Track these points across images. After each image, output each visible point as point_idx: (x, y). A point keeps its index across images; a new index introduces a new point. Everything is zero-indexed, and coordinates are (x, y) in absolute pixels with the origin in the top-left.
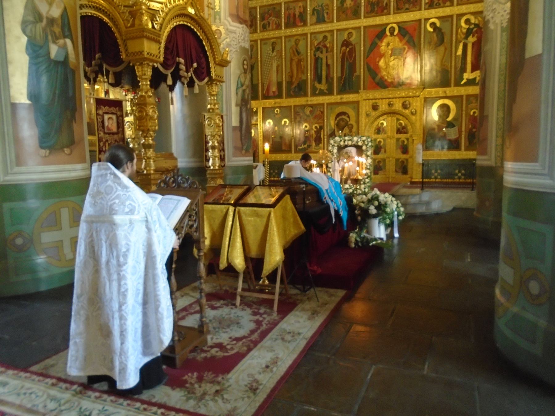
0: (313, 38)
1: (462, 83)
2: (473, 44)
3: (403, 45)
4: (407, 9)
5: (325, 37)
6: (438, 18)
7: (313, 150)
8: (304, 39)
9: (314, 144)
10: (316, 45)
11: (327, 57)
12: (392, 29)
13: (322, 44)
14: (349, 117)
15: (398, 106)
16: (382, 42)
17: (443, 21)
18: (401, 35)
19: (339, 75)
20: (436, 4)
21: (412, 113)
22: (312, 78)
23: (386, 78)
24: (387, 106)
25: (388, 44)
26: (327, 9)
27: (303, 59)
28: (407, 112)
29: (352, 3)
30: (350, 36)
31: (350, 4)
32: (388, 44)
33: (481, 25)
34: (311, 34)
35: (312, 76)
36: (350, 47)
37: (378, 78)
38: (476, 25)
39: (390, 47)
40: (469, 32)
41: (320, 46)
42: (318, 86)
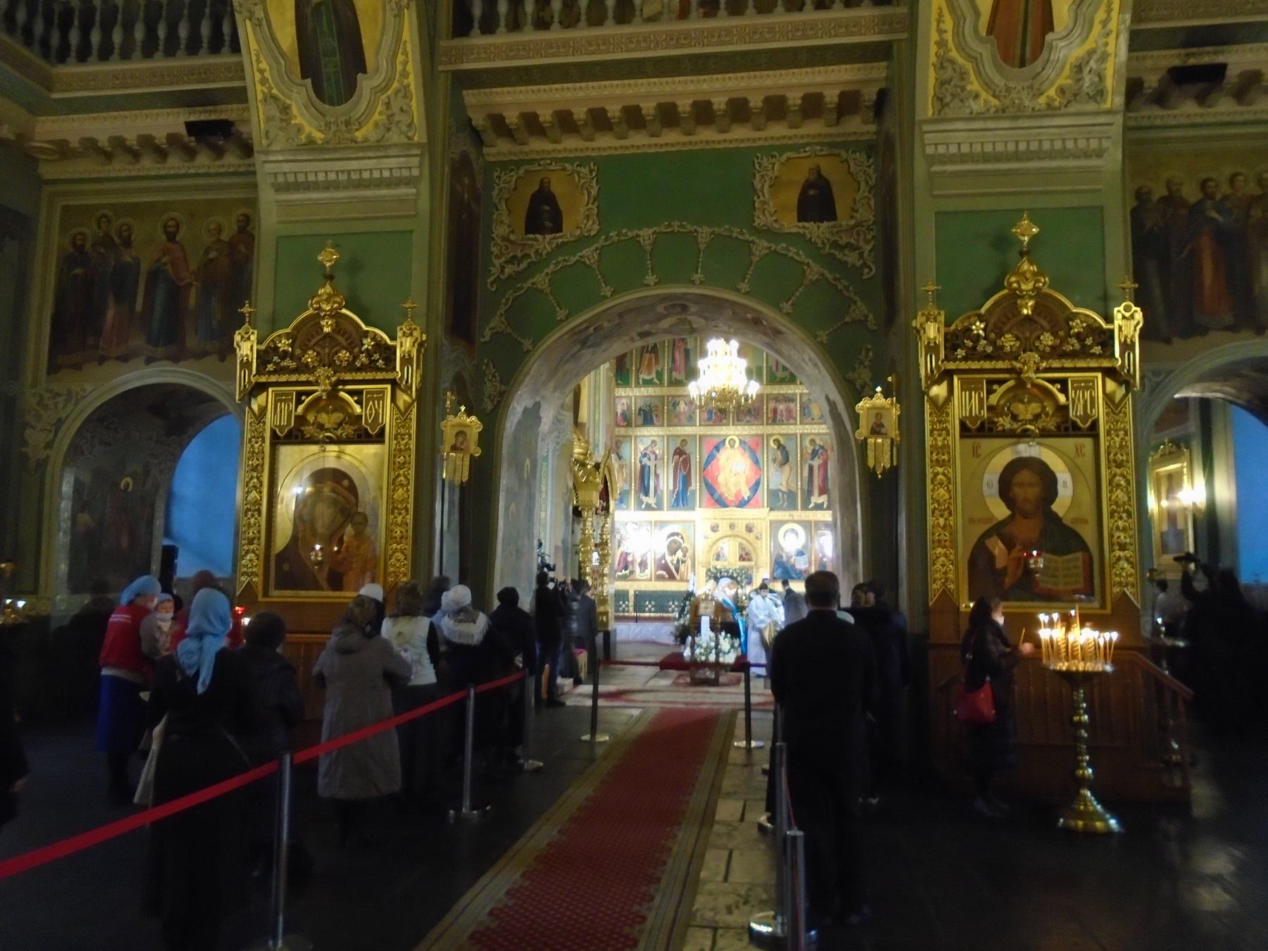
1: (811, 506)
4: (748, 422)
5: (653, 442)
6: (781, 435)
7: (637, 577)
9: (637, 569)
10: (642, 449)
13: (650, 449)
14: (682, 538)
15: (741, 528)
17: (787, 439)
19: (671, 487)
21: (757, 538)
24: (728, 529)
28: (751, 535)
29: (686, 408)
33: (825, 447)
37: (716, 496)
38: (822, 447)
40: (814, 454)
41: (648, 452)
42: (645, 499)
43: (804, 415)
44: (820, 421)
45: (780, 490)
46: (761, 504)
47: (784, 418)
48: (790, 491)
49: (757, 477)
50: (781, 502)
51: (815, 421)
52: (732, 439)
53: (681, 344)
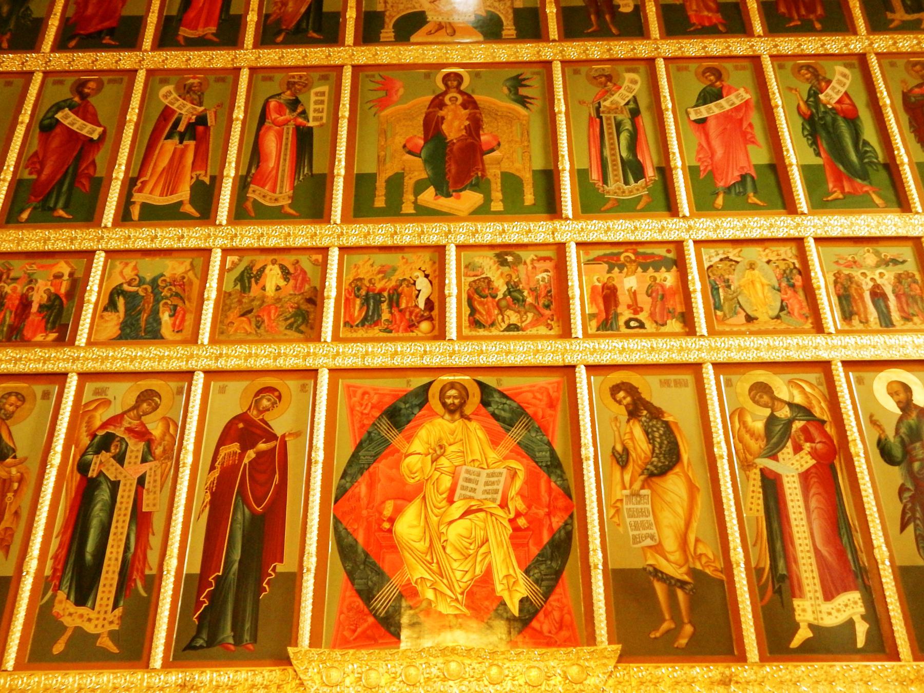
0: (87, 397)
2: (805, 477)
3: (506, 458)
4: (512, 327)
8: (46, 395)
10: (98, 423)
11: (141, 481)
12: (453, 392)
13: (127, 422)
16: (409, 439)
17: (666, 383)
18: (494, 416)
19: (194, 565)
20: (627, 324)
22: (48, 572)
23: (430, 594)
25: (437, 452)
26: (177, 294)
27: (21, 480)
29: (289, 288)
30: (265, 403)
31: (278, 288)
32: (437, 452)
33: (817, 412)
34: (84, 376)
35: (49, 563)
36: (262, 446)
39: (443, 461)
41: (119, 432)
43: (718, 307)
44: (773, 324)
45: (657, 573)
46: (582, 633)
47: (642, 316)
48: (692, 572)
49: (557, 522)
50: (666, 625)
51: (754, 327)
52: (452, 385)
53: (288, 115)
